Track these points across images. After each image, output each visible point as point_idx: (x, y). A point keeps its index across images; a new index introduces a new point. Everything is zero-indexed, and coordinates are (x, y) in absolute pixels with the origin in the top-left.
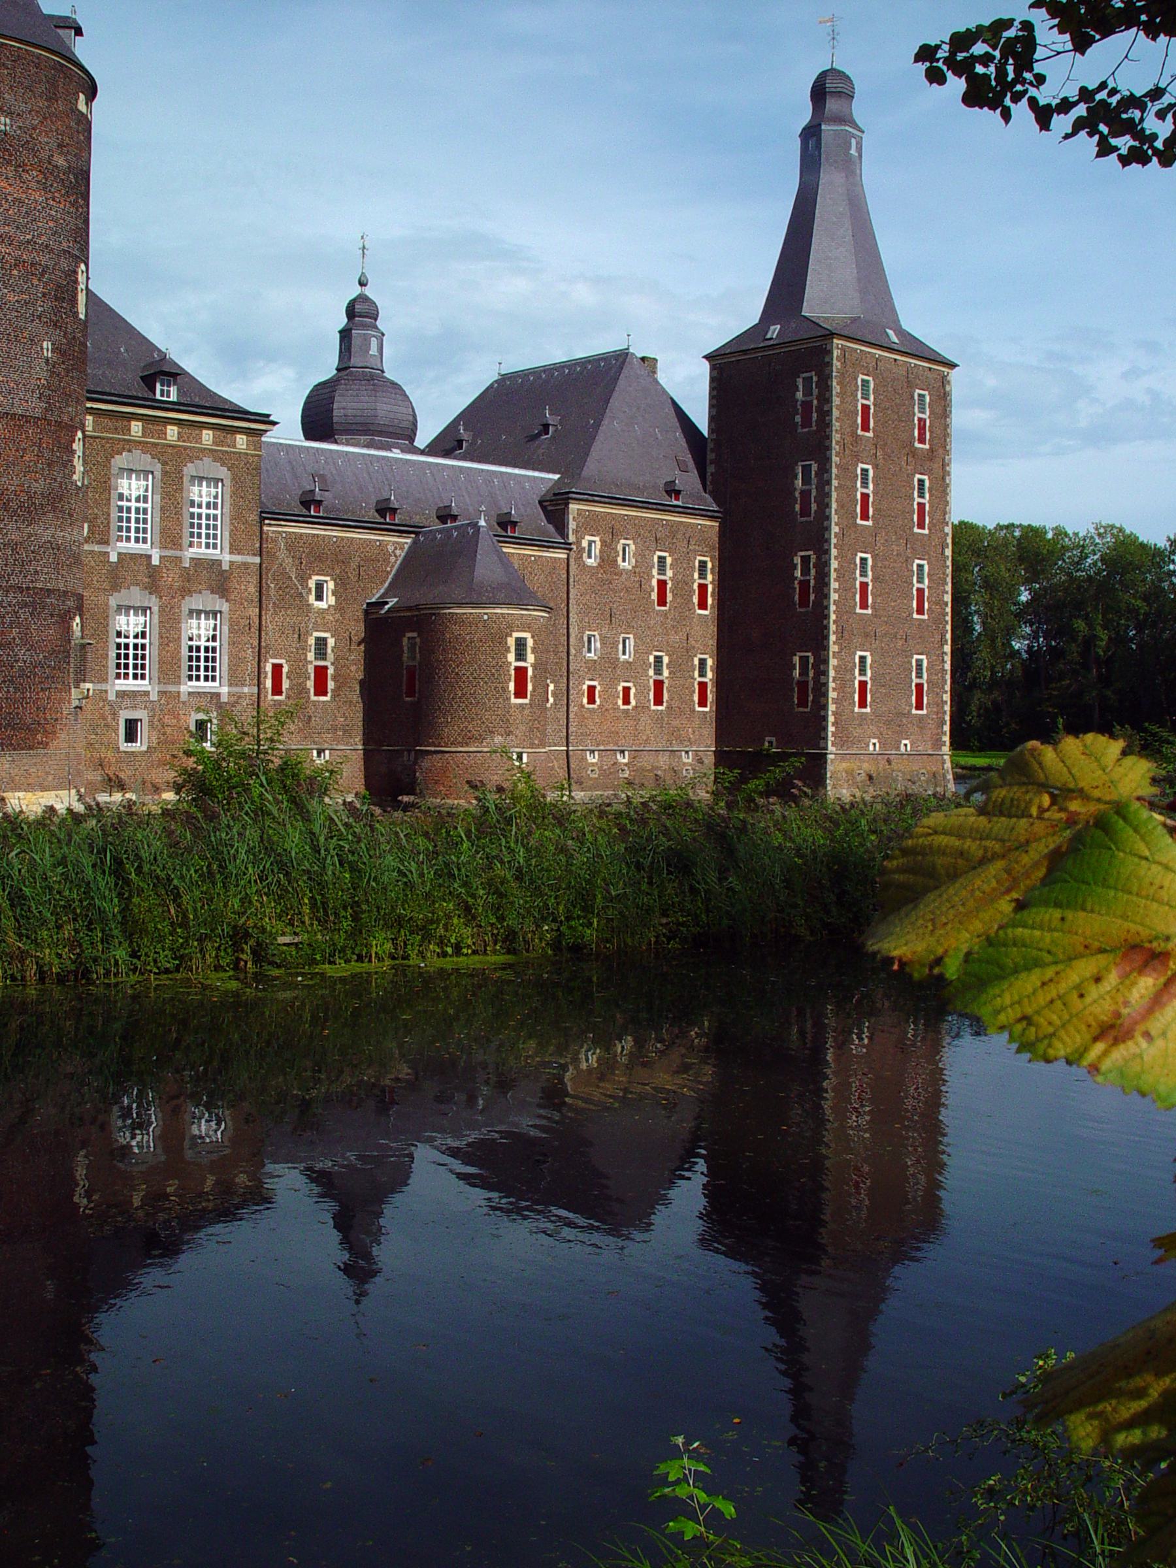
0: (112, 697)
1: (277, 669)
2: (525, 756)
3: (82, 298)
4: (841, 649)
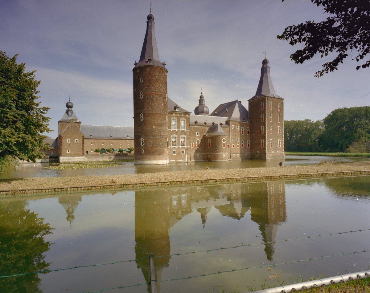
1: (192, 144)
3: (167, 98)
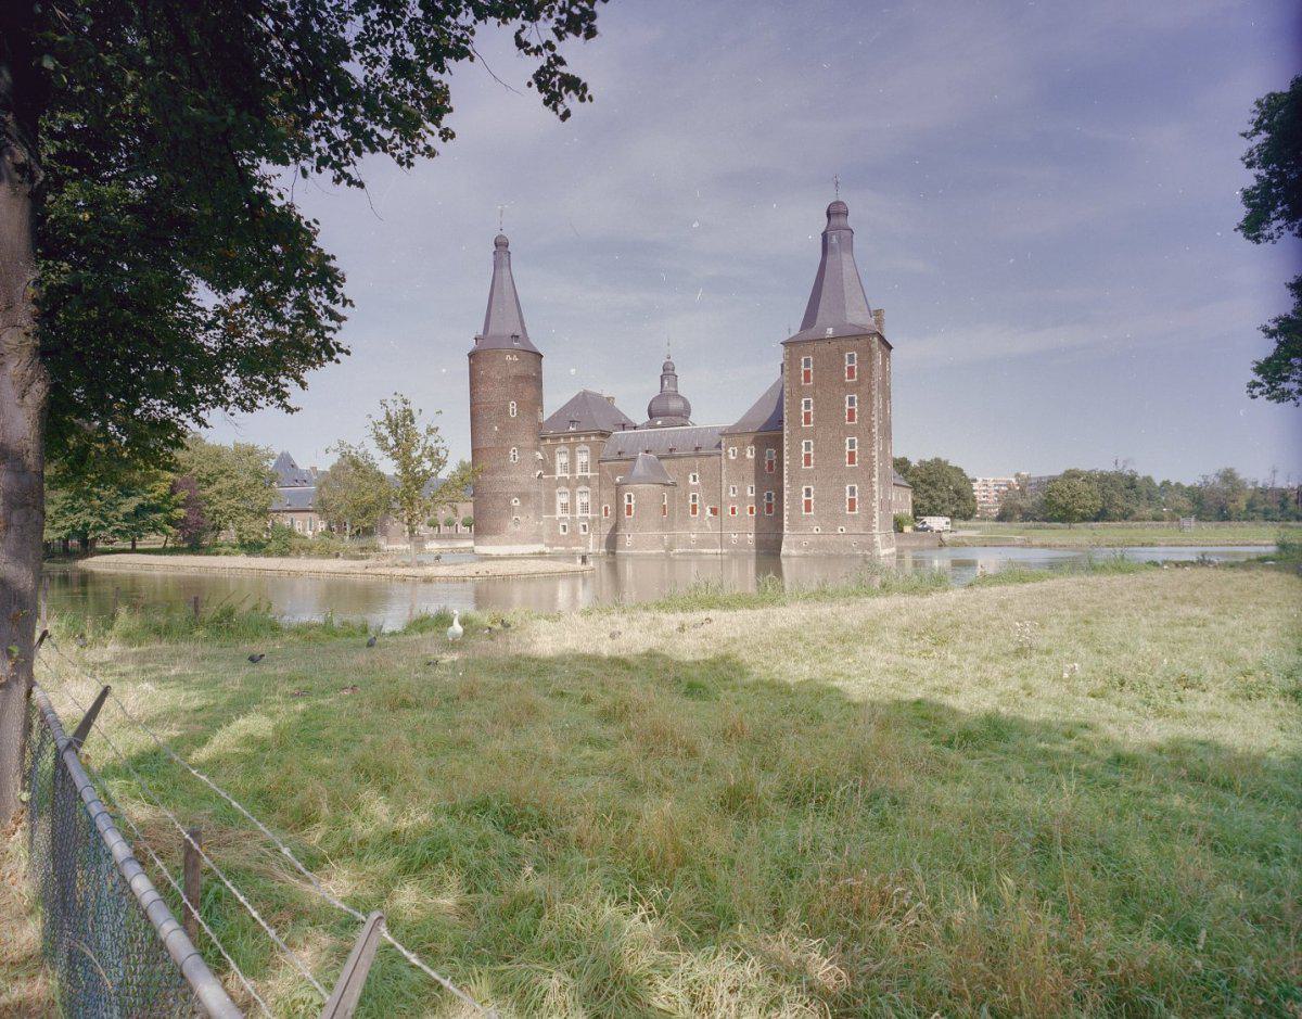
1: (606, 508)
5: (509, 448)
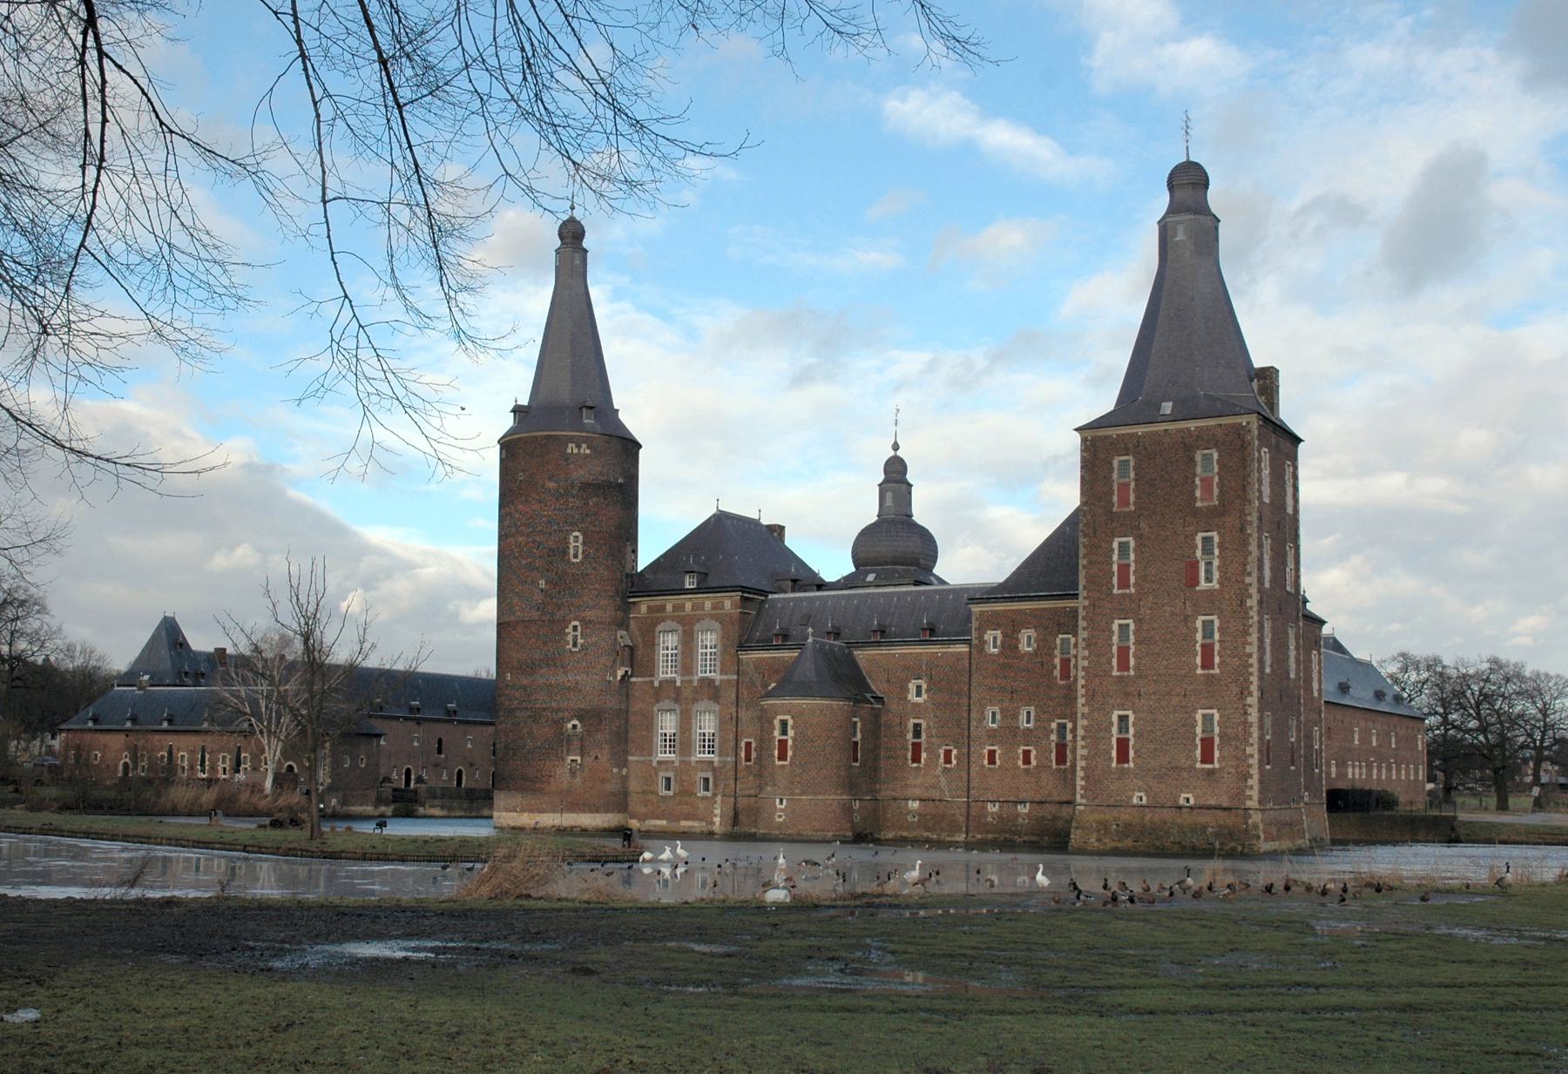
0: (655, 764)
1: (748, 745)
2: (784, 801)
4: (1091, 711)
5: (565, 622)
